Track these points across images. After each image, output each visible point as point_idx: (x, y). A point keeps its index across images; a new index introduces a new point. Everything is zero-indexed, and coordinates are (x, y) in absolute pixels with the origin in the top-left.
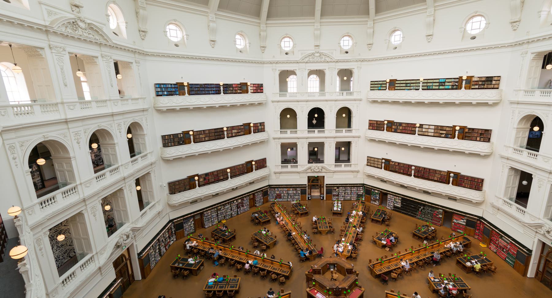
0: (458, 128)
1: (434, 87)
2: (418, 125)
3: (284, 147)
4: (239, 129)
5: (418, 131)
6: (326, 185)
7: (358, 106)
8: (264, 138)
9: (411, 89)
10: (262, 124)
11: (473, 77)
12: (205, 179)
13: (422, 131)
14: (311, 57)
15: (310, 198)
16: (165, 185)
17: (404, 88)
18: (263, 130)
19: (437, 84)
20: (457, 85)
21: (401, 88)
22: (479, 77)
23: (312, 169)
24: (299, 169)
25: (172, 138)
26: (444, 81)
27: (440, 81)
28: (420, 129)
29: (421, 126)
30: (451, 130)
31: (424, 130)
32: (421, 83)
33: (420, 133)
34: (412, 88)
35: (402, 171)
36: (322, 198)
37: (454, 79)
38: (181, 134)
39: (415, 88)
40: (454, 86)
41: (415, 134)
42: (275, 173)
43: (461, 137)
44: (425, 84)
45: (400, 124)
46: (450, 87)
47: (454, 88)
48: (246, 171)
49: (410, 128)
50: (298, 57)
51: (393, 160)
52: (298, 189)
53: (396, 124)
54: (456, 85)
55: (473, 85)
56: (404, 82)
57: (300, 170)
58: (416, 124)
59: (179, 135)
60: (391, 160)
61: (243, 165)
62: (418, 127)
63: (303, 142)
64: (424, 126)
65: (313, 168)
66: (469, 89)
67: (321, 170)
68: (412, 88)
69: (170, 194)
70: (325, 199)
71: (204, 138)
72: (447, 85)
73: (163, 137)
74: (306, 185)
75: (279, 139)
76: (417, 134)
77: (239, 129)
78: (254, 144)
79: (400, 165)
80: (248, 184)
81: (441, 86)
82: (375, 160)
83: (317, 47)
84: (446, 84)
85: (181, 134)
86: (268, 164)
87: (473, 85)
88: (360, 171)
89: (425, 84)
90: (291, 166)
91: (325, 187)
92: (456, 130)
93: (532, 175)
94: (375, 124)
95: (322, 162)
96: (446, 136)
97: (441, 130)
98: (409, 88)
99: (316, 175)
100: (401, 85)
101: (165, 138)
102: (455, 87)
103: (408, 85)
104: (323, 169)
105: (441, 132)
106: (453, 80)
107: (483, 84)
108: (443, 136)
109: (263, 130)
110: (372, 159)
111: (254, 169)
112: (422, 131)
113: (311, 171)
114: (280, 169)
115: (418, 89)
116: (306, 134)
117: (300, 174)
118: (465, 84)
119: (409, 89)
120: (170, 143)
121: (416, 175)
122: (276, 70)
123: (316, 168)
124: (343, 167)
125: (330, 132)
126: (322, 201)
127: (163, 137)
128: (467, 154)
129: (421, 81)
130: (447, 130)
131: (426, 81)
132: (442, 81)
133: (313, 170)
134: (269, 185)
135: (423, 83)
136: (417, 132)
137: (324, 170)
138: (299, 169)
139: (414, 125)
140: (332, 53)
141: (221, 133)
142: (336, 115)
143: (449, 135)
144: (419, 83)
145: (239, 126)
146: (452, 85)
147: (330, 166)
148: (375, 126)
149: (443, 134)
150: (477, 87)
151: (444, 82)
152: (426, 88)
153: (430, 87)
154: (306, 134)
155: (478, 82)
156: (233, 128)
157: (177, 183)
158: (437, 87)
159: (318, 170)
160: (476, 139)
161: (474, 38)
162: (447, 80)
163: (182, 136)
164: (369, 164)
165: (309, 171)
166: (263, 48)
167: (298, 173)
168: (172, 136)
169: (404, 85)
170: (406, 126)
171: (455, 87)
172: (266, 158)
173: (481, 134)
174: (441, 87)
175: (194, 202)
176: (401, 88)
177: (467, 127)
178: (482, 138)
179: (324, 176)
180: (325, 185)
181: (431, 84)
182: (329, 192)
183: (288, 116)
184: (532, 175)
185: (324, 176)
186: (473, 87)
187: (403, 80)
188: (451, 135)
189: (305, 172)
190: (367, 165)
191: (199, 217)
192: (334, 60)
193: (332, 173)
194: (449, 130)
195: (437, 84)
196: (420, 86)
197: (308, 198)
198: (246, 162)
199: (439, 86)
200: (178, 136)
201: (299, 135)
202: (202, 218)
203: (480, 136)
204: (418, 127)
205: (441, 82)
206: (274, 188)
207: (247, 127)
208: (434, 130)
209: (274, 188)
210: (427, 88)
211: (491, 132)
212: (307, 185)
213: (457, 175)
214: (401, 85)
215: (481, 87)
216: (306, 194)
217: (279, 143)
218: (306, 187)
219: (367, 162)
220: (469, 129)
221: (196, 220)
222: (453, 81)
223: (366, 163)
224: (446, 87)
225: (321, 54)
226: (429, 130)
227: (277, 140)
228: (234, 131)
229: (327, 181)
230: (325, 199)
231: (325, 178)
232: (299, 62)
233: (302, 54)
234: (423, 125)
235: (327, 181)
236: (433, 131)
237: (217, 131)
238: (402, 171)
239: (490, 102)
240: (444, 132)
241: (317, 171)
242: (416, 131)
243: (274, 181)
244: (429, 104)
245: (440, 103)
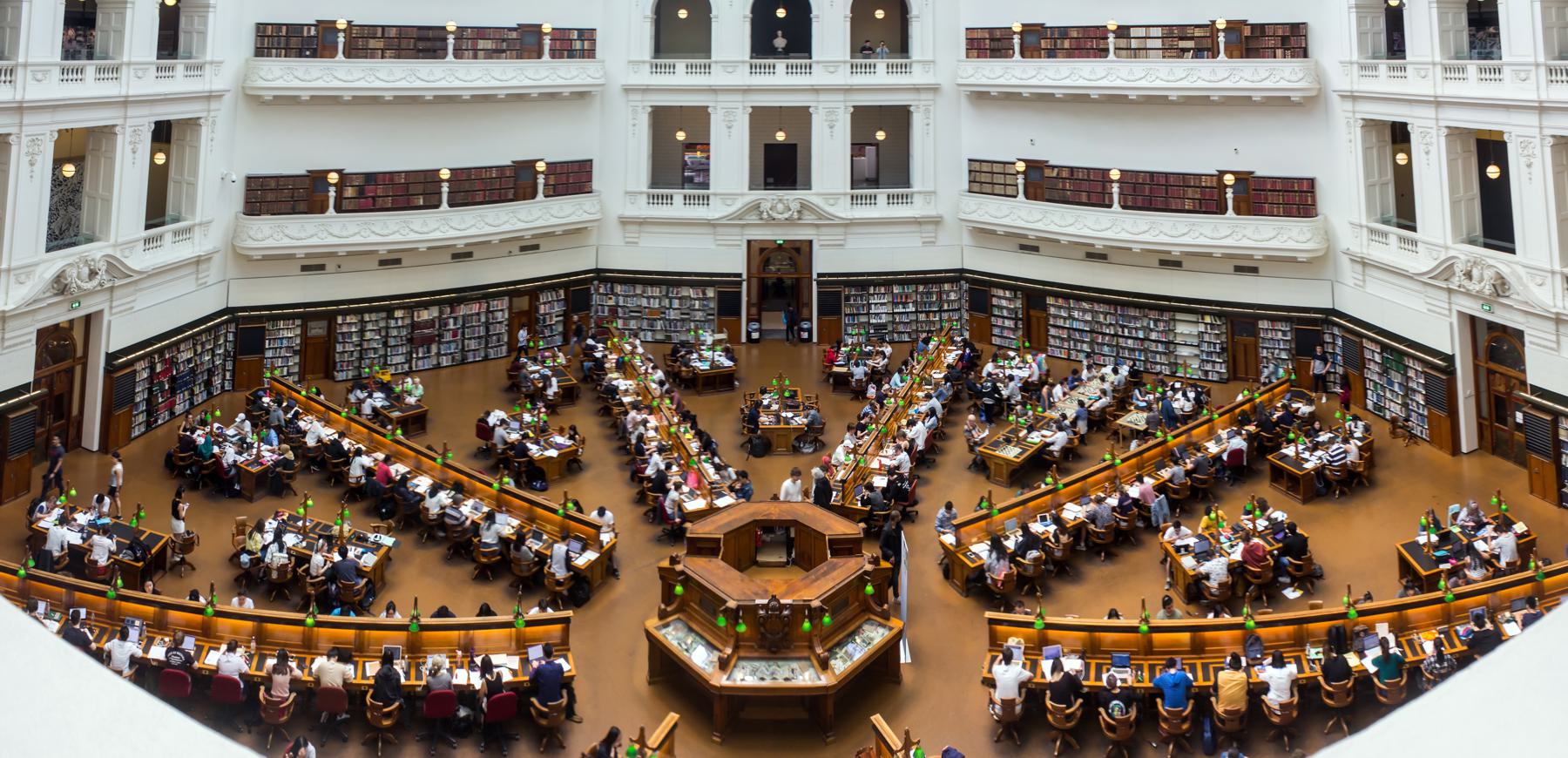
3: (663, 120)
4: (504, 40)
5: (1116, 49)
6: (820, 275)
8: (589, 81)
10: (587, 35)
12: (361, 191)
15: (755, 335)
16: (234, 178)
18: (590, 53)
23: (761, 209)
24: (716, 210)
25: (284, 34)
28: (1123, 43)
29: (1123, 32)
31: (1134, 43)
35: (1084, 200)
36: (805, 335)
38: (313, 28)
42: (625, 222)
45: (1064, 32)
48: (511, 197)
51: (1052, 162)
52: (711, 293)
53: (1052, 34)
57: (717, 216)
59: (306, 28)
60: (1047, 162)
61: (501, 168)
63: (730, 105)
64: (1133, 32)
65: (766, 206)
67: (796, 215)
69: (245, 214)
70: (815, 339)
71: (380, 52)
73: (261, 28)
74: (739, 275)
75: (646, 90)
77: (504, 40)
78: (551, 97)
79: (1075, 174)
80: (516, 250)
82: (997, 168)
85: (313, 28)
86: (596, 184)
88: (945, 216)
90: (685, 197)
91: (814, 283)
93: (1405, 124)
94: (987, 41)
95: (808, 186)
97: (1182, 39)
99: (780, 236)
101: (265, 31)
104: (806, 212)
105: (1183, 44)
109: (590, 53)
110: (985, 167)
111: (541, 188)
113: (761, 219)
114: (643, 209)
117: (720, 230)
120: (277, 49)
121: (1130, 204)
123: (780, 207)
124: (881, 206)
125: (832, 69)
126: (805, 350)
127: (261, 28)
133: (765, 215)
134: (597, 271)
137: (809, 218)
138: (716, 210)
139: (1100, 32)
141: (439, 44)
142: (852, 12)
145: (504, 28)
147: (832, 202)
148: (987, 47)
156: (481, 33)
157: (273, 184)
159: (786, 216)
163: (313, 32)
164: (976, 187)
165: (753, 219)
167: (711, 224)
168: (284, 28)
172: (591, 161)
173: (1284, 39)
175: (314, 265)
178: (1288, 49)
179: (811, 242)
180: (815, 276)
182: (831, 305)
183: (683, 14)
184: (1405, 124)
185: (811, 242)
189: (735, 221)
190: (970, 192)
191: (321, 331)
193: (841, 230)
197: (749, 334)
198: (513, 162)
200: (302, 32)
201: (718, 78)
202: (329, 340)
203: (1283, 44)
206: (614, 281)
207: (532, 40)
209: (614, 281)
211: (1306, 28)
212: (745, 277)
213: (1243, 178)
216: (738, 314)
217: (644, 108)
218: (740, 283)
219: (970, 182)
220: (1253, 26)
221: (312, 338)
223: (966, 186)
226: (1150, 43)
227: (638, 97)
228: (482, 44)
229: (824, 262)
230: (815, 339)
231: (815, 247)
234: (1128, 27)
235: (824, 262)
237: (425, 33)
238: (1084, 200)
240: (1190, 44)
241: (780, 216)
243: (621, 257)
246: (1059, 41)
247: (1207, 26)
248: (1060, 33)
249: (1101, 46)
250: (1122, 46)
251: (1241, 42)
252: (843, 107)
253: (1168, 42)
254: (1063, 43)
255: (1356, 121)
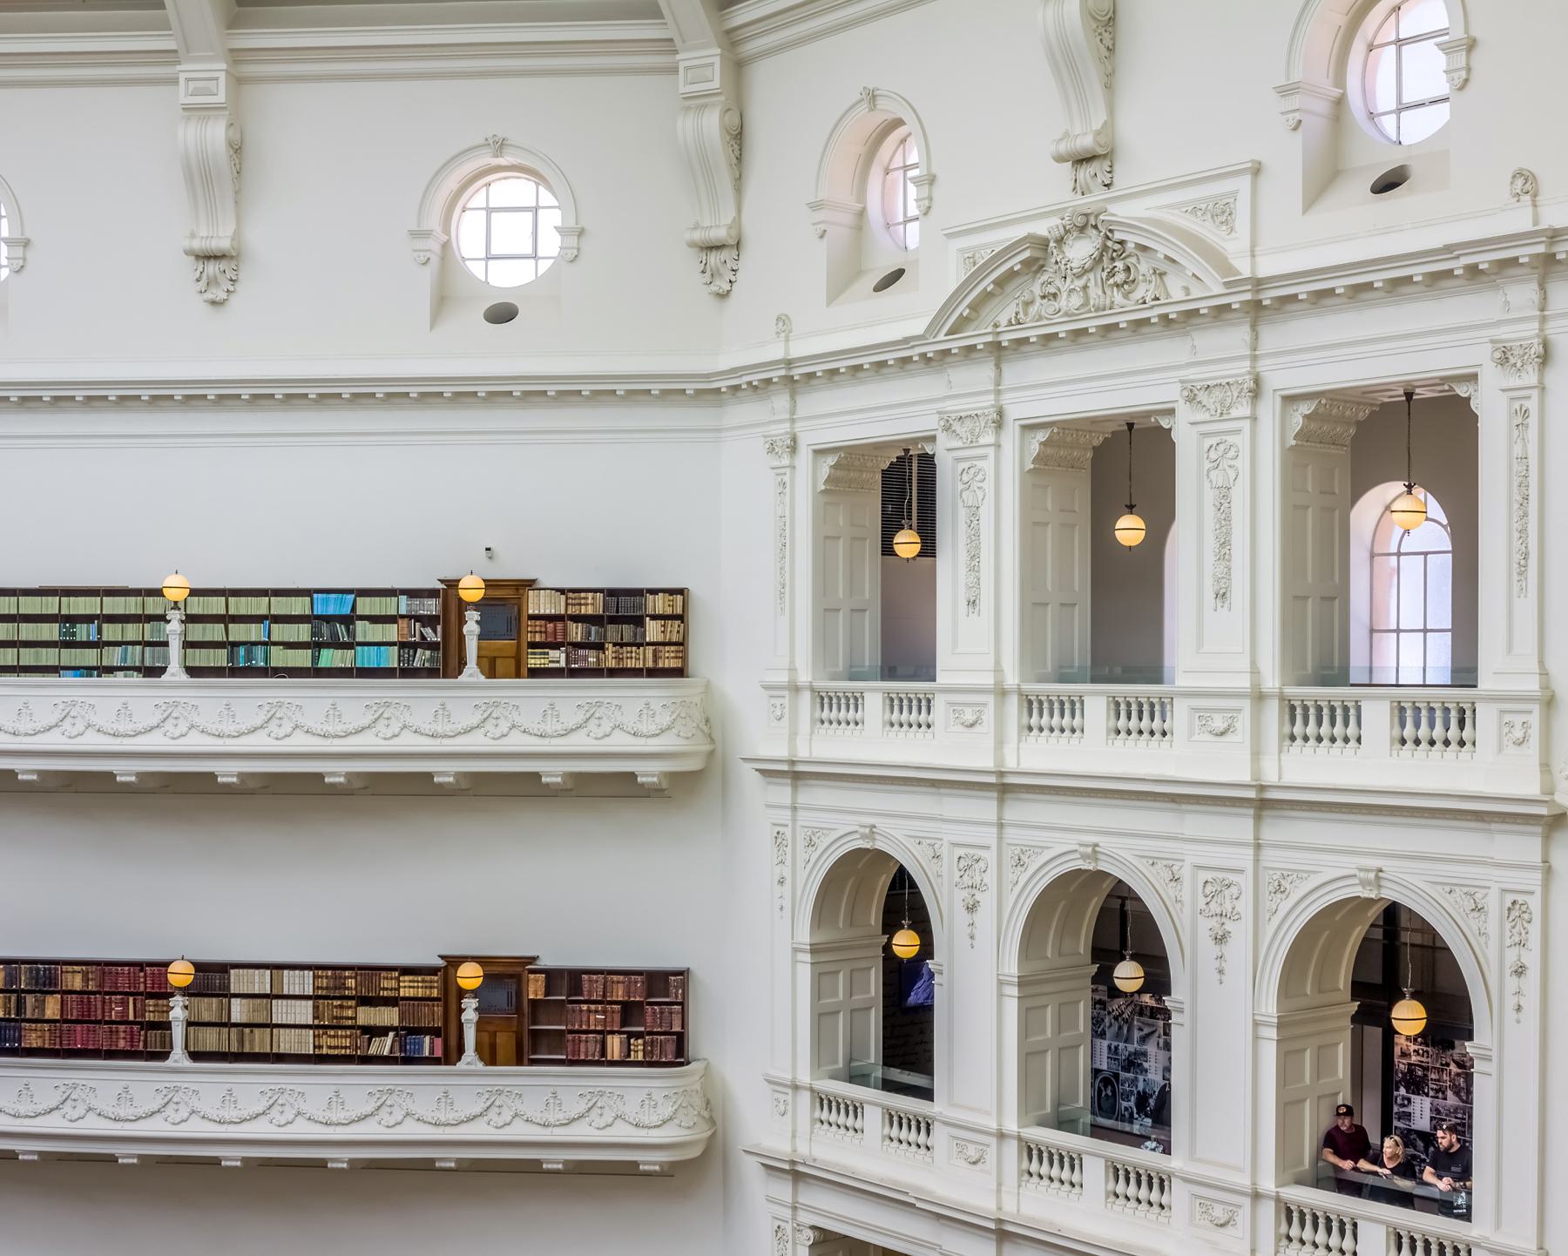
0: (469, 976)
1: (280, 658)
2: (180, 974)
5: (189, 1024)
9: (110, 670)
11: (530, 584)
13: (229, 1025)
17: (48, 657)
19: (303, 632)
20: (433, 646)
21: (28, 657)
22: (562, 591)
26: (346, 611)
27: (319, 610)
28: (208, 1008)
30: (435, 993)
32: (175, 616)
33: (210, 1039)
34: (113, 657)
37: (412, 594)
39: (134, 655)
40: (414, 646)
41: (163, 1056)
43: (505, 1041)
44: (215, 632)
46: (390, 658)
47: (417, 664)
49: (125, 1004)
54: (424, 644)
55: (533, 645)
56: (50, 605)
58: (166, 964)
62: (187, 992)
64: (239, 981)
66: (518, 675)
68: (113, 657)
72: (370, 639)
76: (178, 1056)
81: (328, 645)
84: (364, 631)
87: (533, 645)
89: (215, 632)
92: (462, 993)
96: (403, 1048)
97: (365, 1001)
98: (89, 657)
100: (28, 631)
102: (422, 658)
103: (83, 632)
105: (367, 1016)
106: (404, 605)
107: (592, 639)
108: (385, 1045)
112: (229, 1025)
115: (155, 672)
118: (481, 637)
119: (88, 671)
128: (557, 1172)
129: (176, 606)
130: (410, 993)
131: (216, 606)
132: (331, 611)
135: (191, 619)
136: (178, 1032)
143: (427, 1039)
144: (162, 618)
146: (403, 645)
149: (382, 1031)
150: (558, 657)
151: (348, 620)
152: (220, 658)
153: (249, 657)
155: (560, 625)
158: (302, 658)
160: (603, 1053)
161: (502, 314)
162: (366, 606)
169: (50, 632)
170: (92, 986)
171: (422, 658)
173: (629, 1012)
174: (329, 658)
176: (28, 657)
177: (533, 959)
178: (638, 1035)
181: (254, 632)
186: (534, 662)
187: (35, 585)
188: (435, 1032)
194: (420, 993)
195: (303, 632)
196: (166, 644)
199: (316, 646)
203: (624, 1023)
204: (187, 992)
205: (328, 619)
208: (316, 1008)
210: (231, 658)
211: (684, 985)
214: (28, 631)
215: (586, 658)
220: (552, 976)
222: (403, 611)
224: (367, 658)
226: (283, 1012)
234: (224, 968)
236: (303, 1012)
239: (648, 772)
240: (388, 1016)
242: (166, 1026)
244: (252, 793)
245: (332, 785)
246: (30, 1000)
247: (432, 971)
248: (35, 978)
249: (149, 1017)
250: (206, 1018)
251: (519, 1010)
253: (330, 1010)
254: (41, 1006)
255: (798, 1229)
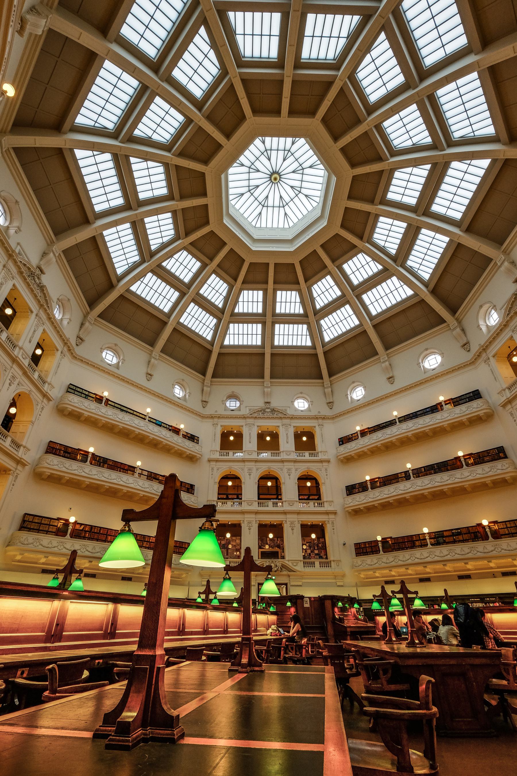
7: (326, 470)
14: (261, 413)
50: (245, 412)
83: (268, 404)
104: (284, 569)
116: (255, 507)
122: (217, 425)
140: (286, 410)
147: (295, 564)
154: (255, 507)
166: (205, 403)
192: (288, 416)
201: (245, 507)
225: (273, 411)
232: (246, 416)
233: (250, 410)
252: (297, 521)
